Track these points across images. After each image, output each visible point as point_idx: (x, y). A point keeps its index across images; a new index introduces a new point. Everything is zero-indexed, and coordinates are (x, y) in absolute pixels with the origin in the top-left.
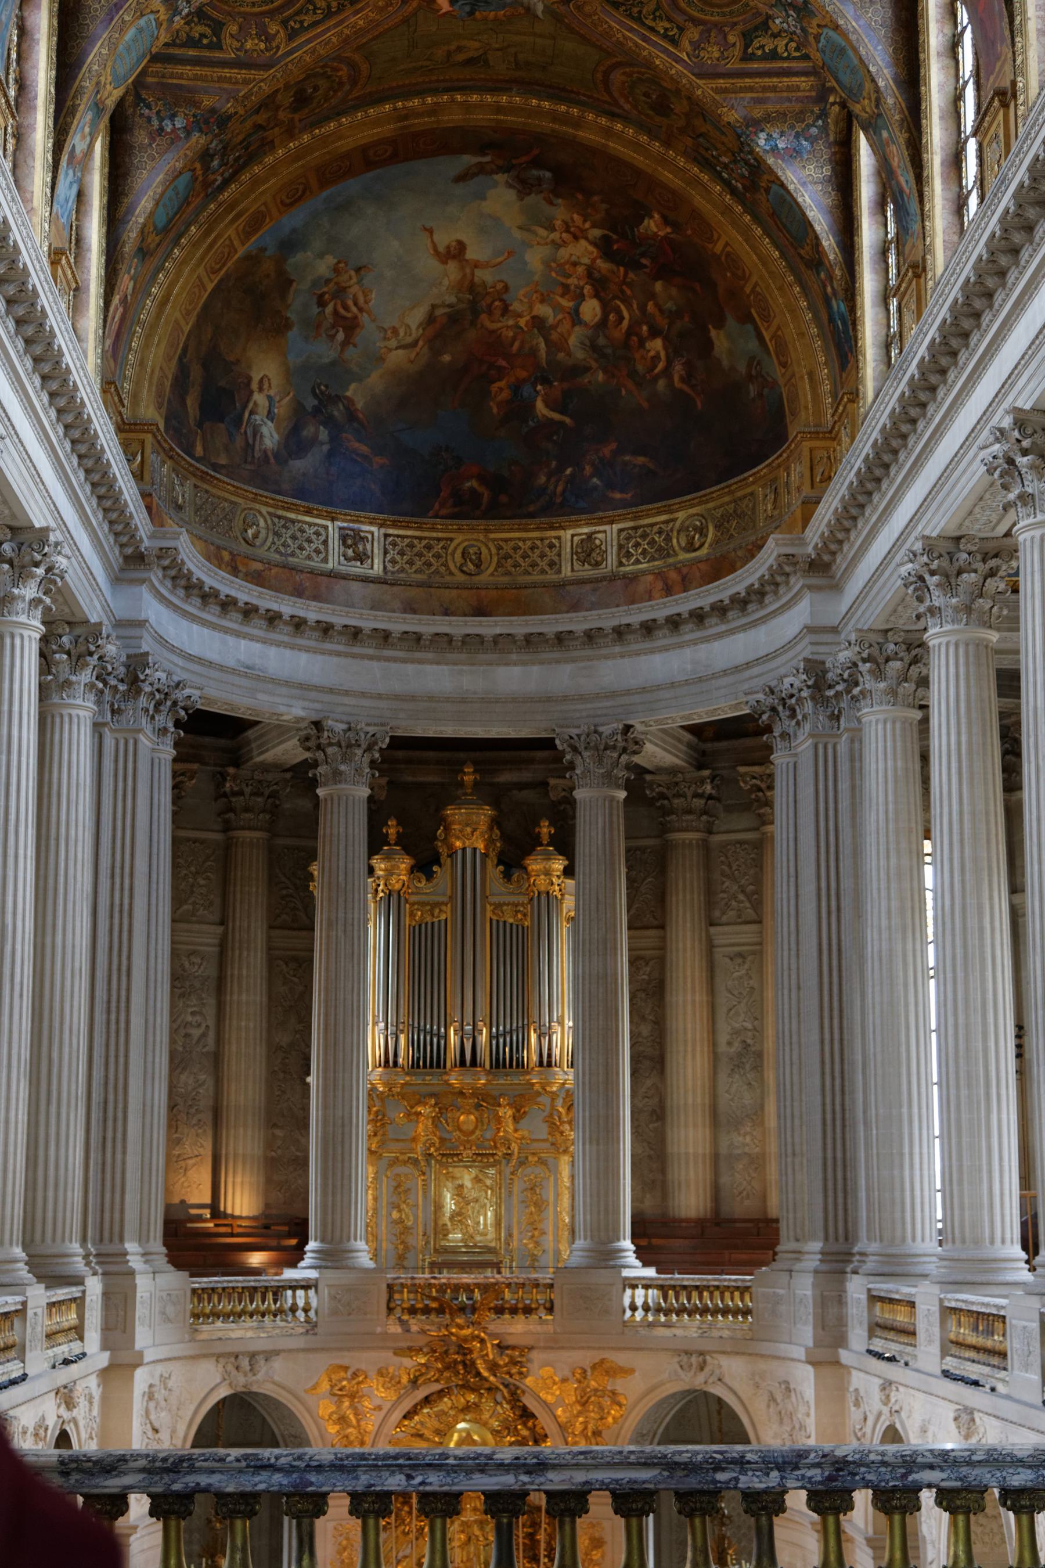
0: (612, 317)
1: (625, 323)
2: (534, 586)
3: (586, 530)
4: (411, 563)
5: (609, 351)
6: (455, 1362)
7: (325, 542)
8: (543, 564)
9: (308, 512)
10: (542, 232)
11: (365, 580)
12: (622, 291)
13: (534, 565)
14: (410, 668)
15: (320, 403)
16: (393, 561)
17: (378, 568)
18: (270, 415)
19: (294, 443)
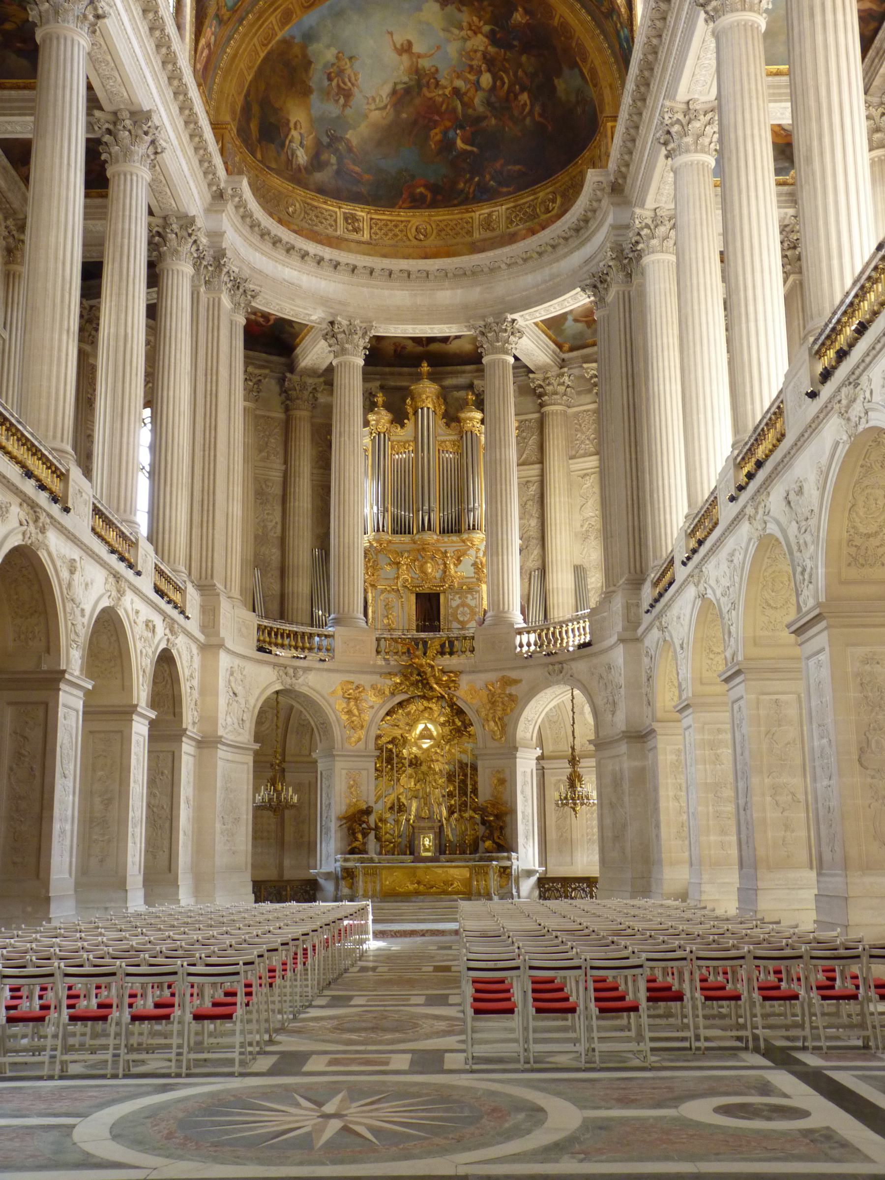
0: (498, 83)
1: (506, 86)
2: (457, 244)
3: (487, 211)
4: (386, 234)
5: (497, 105)
6: (418, 681)
7: (336, 221)
8: (463, 232)
9: (325, 203)
10: (456, 31)
11: (359, 242)
12: (504, 66)
13: (457, 234)
14: (386, 292)
15: (329, 140)
16: (376, 234)
17: (366, 236)
18: (301, 145)
19: (316, 163)
